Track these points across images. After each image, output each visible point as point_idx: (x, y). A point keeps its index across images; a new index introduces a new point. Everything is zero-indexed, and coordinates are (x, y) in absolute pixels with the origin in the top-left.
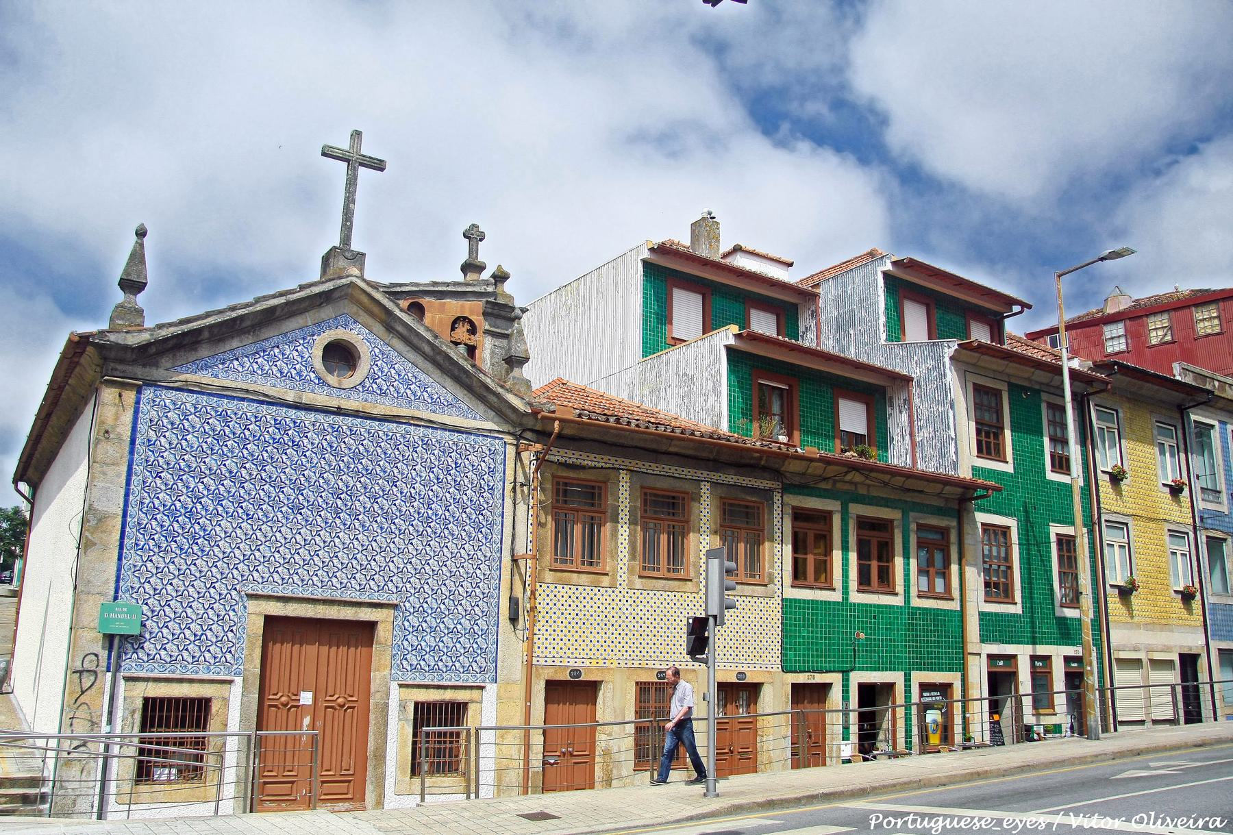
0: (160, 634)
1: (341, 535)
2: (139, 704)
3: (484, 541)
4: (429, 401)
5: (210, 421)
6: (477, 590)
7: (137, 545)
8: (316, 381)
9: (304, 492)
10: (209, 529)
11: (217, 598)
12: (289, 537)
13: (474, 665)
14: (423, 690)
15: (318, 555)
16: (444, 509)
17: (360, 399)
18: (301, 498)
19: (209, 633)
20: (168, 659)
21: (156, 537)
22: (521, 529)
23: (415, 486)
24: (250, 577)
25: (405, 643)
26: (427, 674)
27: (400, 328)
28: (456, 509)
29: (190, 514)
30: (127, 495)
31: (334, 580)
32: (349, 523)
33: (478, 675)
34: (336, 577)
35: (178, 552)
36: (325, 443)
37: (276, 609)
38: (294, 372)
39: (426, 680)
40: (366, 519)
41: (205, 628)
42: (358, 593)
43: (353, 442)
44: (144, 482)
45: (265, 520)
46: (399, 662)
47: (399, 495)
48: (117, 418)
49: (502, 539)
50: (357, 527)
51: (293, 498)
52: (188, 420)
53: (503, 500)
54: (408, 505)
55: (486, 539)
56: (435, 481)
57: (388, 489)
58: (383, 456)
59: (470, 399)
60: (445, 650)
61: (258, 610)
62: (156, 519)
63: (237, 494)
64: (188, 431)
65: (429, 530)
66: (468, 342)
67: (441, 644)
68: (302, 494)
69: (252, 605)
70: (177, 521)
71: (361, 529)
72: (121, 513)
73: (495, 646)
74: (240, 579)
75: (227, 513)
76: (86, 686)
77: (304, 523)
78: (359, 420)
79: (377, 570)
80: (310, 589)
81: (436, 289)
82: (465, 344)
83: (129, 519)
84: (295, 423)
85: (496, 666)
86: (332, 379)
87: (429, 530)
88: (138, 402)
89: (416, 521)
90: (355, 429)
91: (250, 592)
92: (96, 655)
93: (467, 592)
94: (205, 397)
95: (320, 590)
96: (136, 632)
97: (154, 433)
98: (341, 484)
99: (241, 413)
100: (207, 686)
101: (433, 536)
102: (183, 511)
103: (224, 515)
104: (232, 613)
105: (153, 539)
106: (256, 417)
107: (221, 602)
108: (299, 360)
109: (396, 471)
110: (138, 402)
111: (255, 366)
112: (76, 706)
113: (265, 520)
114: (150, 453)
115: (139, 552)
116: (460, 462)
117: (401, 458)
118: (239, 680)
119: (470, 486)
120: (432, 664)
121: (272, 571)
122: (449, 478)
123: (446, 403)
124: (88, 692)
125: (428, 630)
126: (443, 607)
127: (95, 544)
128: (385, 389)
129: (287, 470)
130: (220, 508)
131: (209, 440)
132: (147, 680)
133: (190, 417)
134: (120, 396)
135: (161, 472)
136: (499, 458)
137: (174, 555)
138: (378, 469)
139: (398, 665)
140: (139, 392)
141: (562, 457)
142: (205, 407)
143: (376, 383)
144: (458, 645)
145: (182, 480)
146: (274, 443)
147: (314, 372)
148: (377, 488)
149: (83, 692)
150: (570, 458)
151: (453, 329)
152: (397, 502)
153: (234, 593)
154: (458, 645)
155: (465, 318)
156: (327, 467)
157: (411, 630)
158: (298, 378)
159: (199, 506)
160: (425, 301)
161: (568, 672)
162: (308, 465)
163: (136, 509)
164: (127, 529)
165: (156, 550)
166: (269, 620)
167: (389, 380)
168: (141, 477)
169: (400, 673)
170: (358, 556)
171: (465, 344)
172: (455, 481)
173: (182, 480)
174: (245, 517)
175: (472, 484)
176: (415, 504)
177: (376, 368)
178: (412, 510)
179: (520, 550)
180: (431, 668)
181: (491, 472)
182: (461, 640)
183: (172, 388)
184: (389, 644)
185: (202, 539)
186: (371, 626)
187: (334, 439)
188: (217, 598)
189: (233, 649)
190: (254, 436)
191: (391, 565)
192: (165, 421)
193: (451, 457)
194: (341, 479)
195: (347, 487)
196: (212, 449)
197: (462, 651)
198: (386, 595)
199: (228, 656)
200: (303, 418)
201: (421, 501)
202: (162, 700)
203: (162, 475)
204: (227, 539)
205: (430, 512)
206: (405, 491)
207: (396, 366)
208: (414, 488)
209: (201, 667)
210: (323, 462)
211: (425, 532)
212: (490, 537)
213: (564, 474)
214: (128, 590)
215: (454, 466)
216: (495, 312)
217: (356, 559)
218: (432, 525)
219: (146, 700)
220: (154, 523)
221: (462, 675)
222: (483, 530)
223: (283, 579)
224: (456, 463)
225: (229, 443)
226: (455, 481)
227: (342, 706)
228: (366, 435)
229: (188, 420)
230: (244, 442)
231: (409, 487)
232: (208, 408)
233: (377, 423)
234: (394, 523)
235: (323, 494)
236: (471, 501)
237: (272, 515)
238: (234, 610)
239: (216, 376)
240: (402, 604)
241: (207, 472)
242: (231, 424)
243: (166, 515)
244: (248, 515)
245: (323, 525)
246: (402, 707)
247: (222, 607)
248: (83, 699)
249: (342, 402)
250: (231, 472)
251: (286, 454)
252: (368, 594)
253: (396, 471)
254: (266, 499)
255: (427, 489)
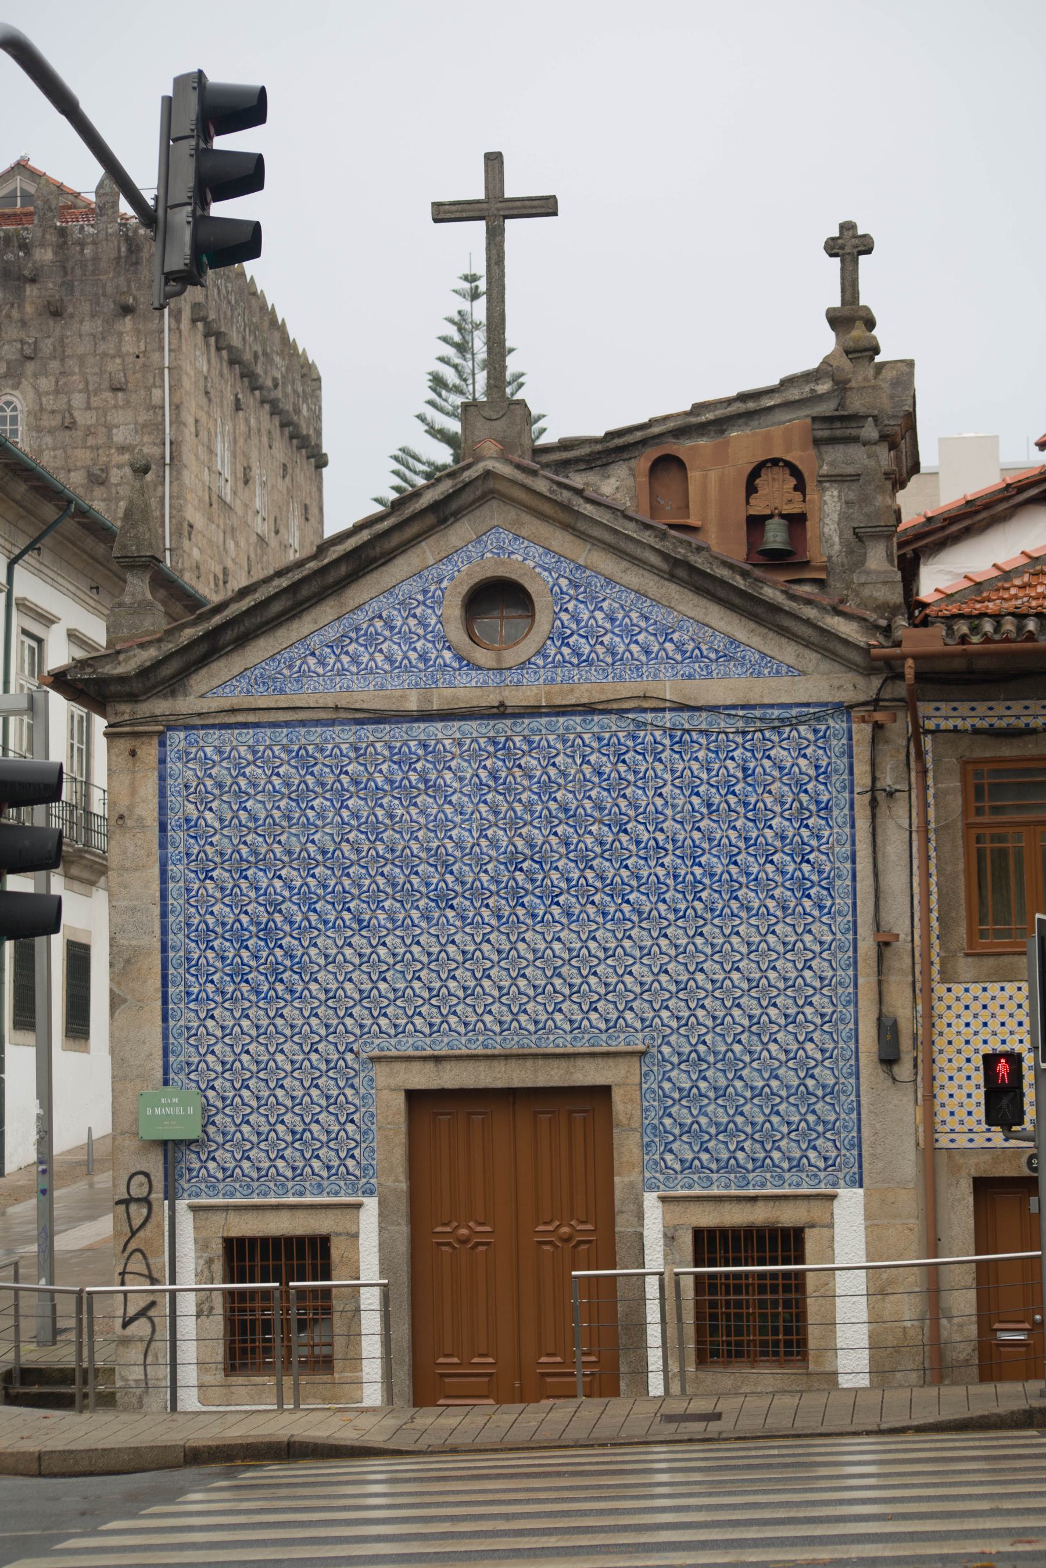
0: (238, 1135)
1: (528, 936)
2: (217, 1248)
3: (816, 913)
4: (679, 657)
5: (282, 770)
6: (808, 1010)
7: (188, 994)
8: (456, 665)
9: (455, 868)
10: (299, 954)
11: (323, 1067)
12: (435, 950)
13: (812, 1154)
14: (709, 1207)
15: (489, 977)
16: (725, 861)
17: (541, 681)
18: (449, 878)
19: (315, 1127)
20: (255, 1175)
21: (216, 977)
22: (895, 880)
23: (665, 826)
24: (375, 1027)
25: (667, 1121)
26: (715, 1176)
27: (597, 532)
28: (751, 859)
29: (267, 932)
30: (164, 915)
31: (523, 1018)
32: (541, 913)
33: (822, 1175)
34: (525, 1011)
35: (253, 998)
36: (483, 774)
37: (423, 1078)
38: (413, 656)
39: (714, 1186)
40: (574, 900)
41: (307, 1120)
42: (569, 1037)
43: (535, 762)
44: (188, 890)
45: (390, 926)
46: (657, 1157)
47: (633, 848)
48: (133, 790)
49: (854, 904)
50: (557, 917)
51: (435, 881)
52: (244, 775)
53: (853, 826)
54: (652, 863)
55: (821, 908)
56: (704, 810)
57: (610, 840)
58: (596, 780)
59: (764, 637)
60: (749, 1129)
61: (393, 1082)
62: (212, 948)
63: (339, 888)
64: (247, 793)
65: (698, 905)
66: (787, 509)
67: (739, 1119)
68: (451, 873)
69: (381, 1074)
70: (247, 948)
71: (564, 920)
72: (158, 945)
73: (854, 1116)
74: (358, 1031)
75: (326, 922)
76: (137, 1223)
77: (459, 923)
78: (544, 720)
79: (602, 991)
80: (481, 1038)
81: (703, 419)
82: (783, 516)
83: (171, 954)
84: (425, 746)
85: (860, 1155)
86: (482, 656)
87: (698, 905)
88: (162, 761)
89: (671, 893)
90: (537, 738)
91: (376, 1053)
92: (147, 1175)
93: (786, 1016)
94: (268, 731)
95: (498, 1039)
96: (195, 1133)
97: (193, 807)
98: (520, 843)
99: (330, 747)
100: (322, 1214)
101: (708, 916)
102: (253, 929)
103: (321, 926)
104: (349, 1092)
105: (212, 982)
106: (357, 749)
107: (331, 1074)
108: (421, 632)
109: (623, 803)
110: (162, 761)
111: (345, 659)
112: (126, 1254)
113: (390, 926)
114: (192, 841)
115: (192, 1006)
116: (752, 765)
117: (631, 778)
118: (371, 1204)
119: (778, 809)
120: (725, 1155)
121: (410, 1013)
122: (732, 799)
123: (713, 656)
124: (141, 1234)
125: (712, 1094)
126: (737, 1048)
127: (125, 1001)
128: (586, 652)
129: (420, 834)
130: (313, 917)
131: (283, 804)
132: (226, 1208)
133: (247, 770)
134: (133, 753)
135: (213, 870)
136: (837, 745)
137: (247, 1004)
138: (588, 804)
139: (656, 1163)
140: (162, 744)
141: (964, 719)
142: (270, 747)
143: (568, 645)
144: (775, 1119)
145: (246, 878)
146: (393, 790)
147: (449, 648)
148: (589, 840)
149: (134, 1233)
150: (1001, 718)
151: (751, 489)
152: (630, 862)
153: (349, 1056)
154: (775, 1119)
155: (775, 462)
156: (491, 818)
157: (676, 1096)
158: (421, 666)
159: (278, 917)
160: (682, 448)
161: (1024, 1160)
162: (458, 819)
163: (181, 936)
164: (171, 971)
165: (219, 999)
166: (413, 1097)
167: (592, 635)
168: (181, 884)
169: (661, 1178)
170: (564, 970)
171: (783, 516)
172: (746, 804)
173: (246, 878)
174: (355, 926)
175: (783, 804)
176: (667, 861)
177: (565, 616)
178: (661, 872)
179: (897, 920)
180: (723, 1164)
181: (822, 774)
182: (782, 1108)
183: (213, 726)
184: (635, 1124)
185: (288, 973)
186: (604, 1092)
187: (500, 763)
188: (323, 1067)
189: (356, 1152)
190: (357, 783)
191: (628, 979)
192: (209, 783)
193: (733, 759)
194: (520, 835)
195: (532, 846)
196: (290, 818)
197: (785, 1129)
198: (622, 1036)
199: (350, 1163)
200: (440, 736)
201: (677, 852)
202: (253, 1240)
203: (215, 874)
204: (330, 967)
205: (698, 871)
206: (645, 839)
207: (605, 605)
208: (662, 830)
209: (307, 1184)
210: (483, 808)
211: (690, 911)
212: (829, 904)
213: (988, 754)
214: (181, 1069)
215: (740, 775)
216: (838, 433)
217: (560, 975)
218: (704, 895)
219: (228, 1242)
220: (210, 954)
221: (787, 1175)
222: (813, 892)
223: (431, 1025)
224: (745, 770)
225: (315, 803)
226: (746, 804)
227: (567, 1240)
228: (559, 746)
229: (244, 775)
230: (340, 797)
231: (651, 829)
232: (275, 748)
233: (578, 719)
234: (628, 902)
235: (490, 867)
236: (783, 838)
237: (401, 917)
238: (352, 1086)
239: (282, 691)
240: (654, 1050)
241: (286, 859)
242: (316, 769)
243: (227, 940)
244: (360, 922)
245: (494, 922)
246: (670, 1238)
247: (332, 1082)
248: (132, 1246)
249: (506, 693)
250: (324, 853)
251: (415, 805)
252: (587, 1037)
253: (623, 803)
254: (389, 890)
255: (688, 828)
